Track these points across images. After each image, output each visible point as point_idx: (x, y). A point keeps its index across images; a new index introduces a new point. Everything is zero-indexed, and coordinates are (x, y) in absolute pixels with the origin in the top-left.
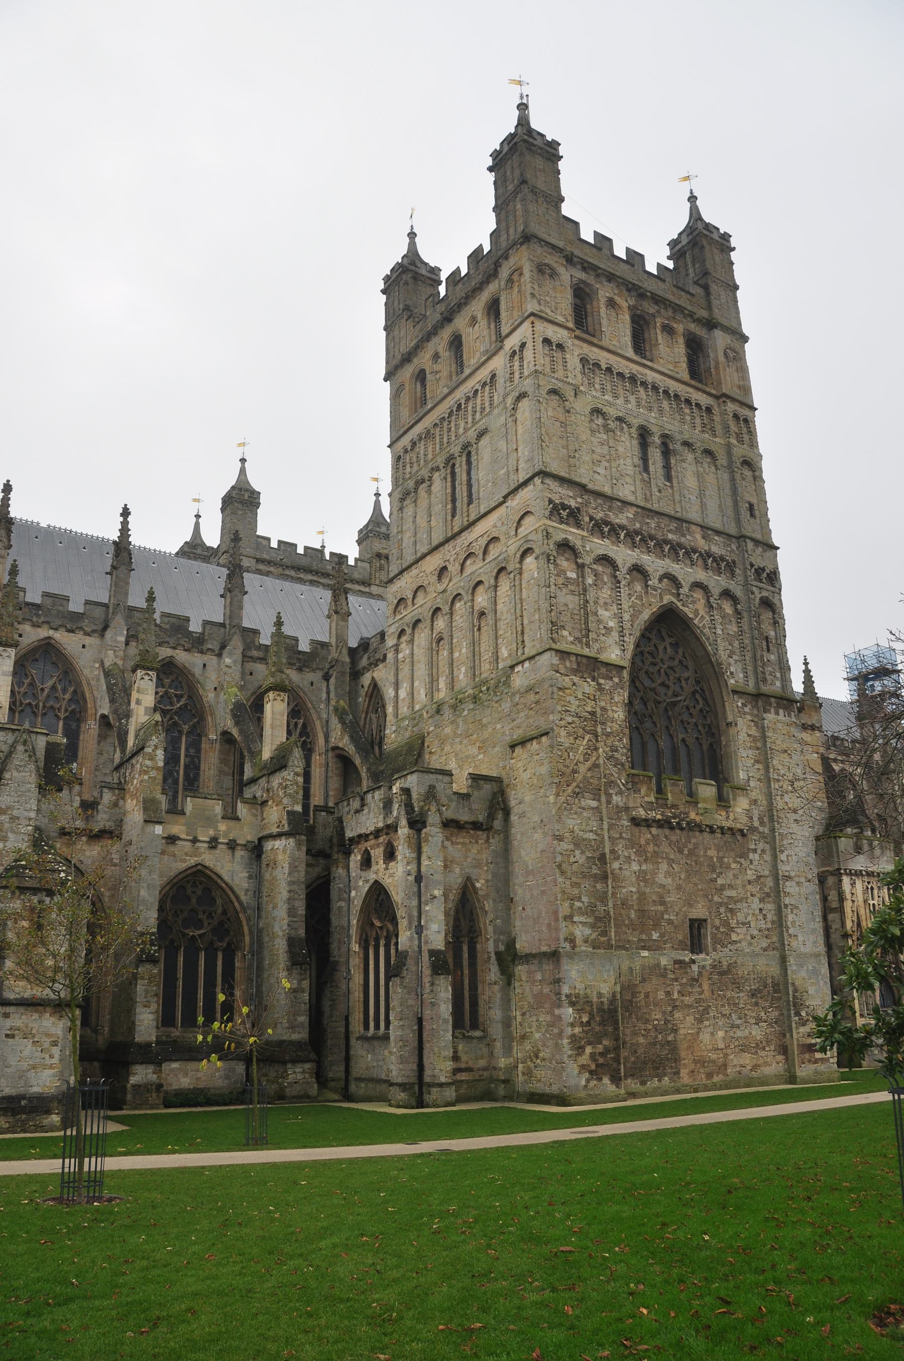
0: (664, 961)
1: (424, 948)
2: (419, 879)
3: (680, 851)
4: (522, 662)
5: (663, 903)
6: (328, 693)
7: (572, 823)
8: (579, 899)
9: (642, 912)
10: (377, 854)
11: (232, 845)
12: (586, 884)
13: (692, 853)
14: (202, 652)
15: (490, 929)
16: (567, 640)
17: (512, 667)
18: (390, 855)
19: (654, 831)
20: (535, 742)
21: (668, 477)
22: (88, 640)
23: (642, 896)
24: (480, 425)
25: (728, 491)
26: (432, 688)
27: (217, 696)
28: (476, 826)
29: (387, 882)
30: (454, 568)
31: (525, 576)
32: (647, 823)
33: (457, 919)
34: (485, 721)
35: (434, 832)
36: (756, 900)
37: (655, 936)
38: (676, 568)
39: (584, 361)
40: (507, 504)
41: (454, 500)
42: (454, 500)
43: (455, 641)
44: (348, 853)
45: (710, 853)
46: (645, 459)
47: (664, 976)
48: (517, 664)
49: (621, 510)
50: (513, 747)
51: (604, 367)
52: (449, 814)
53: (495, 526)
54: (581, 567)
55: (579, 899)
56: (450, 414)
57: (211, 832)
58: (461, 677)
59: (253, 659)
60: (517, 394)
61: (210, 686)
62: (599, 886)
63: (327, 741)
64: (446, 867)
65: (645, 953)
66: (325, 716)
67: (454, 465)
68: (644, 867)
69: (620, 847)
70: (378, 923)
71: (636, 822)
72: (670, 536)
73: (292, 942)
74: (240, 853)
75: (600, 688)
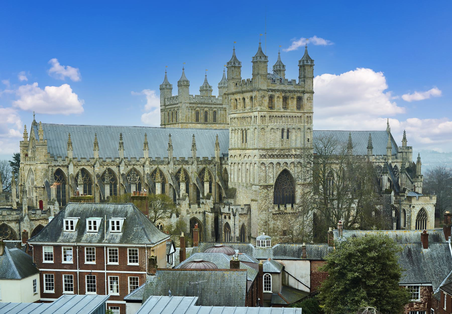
0: (277, 238)
1: (236, 236)
2: (235, 225)
3: (282, 218)
5: (278, 228)
6: (215, 169)
7: (261, 216)
8: (261, 229)
9: (274, 230)
10: (227, 217)
11: (200, 213)
12: (263, 226)
13: (285, 218)
14: (188, 165)
15: (247, 232)
16: (262, 183)
18: (230, 218)
19: (277, 215)
21: (288, 138)
22: (165, 166)
23: (274, 227)
25: (303, 137)
26: (238, 180)
27: (192, 174)
28: (245, 214)
29: (229, 223)
32: (276, 214)
33: (241, 231)
35: (237, 216)
36: (298, 225)
37: (276, 234)
38: (286, 160)
39: (270, 116)
41: (243, 139)
42: (243, 139)
44: (222, 215)
45: (289, 218)
46: (282, 137)
47: (277, 241)
49: (275, 151)
51: (275, 116)
52: (240, 213)
54: (266, 167)
55: (261, 229)
57: (196, 211)
59: (199, 164)
61: (190, 172)
62: (265, 227)
63: (215, 181)
64: (239, 222)
65: (274, 237)
66: (214, 174)
68: (275, 222)
69: (270, 219)
70: (227, 229)
71: (273, 214)
72: (286, 153)
73: (212, 232)
74: (201, 214)
75: (268, 190)
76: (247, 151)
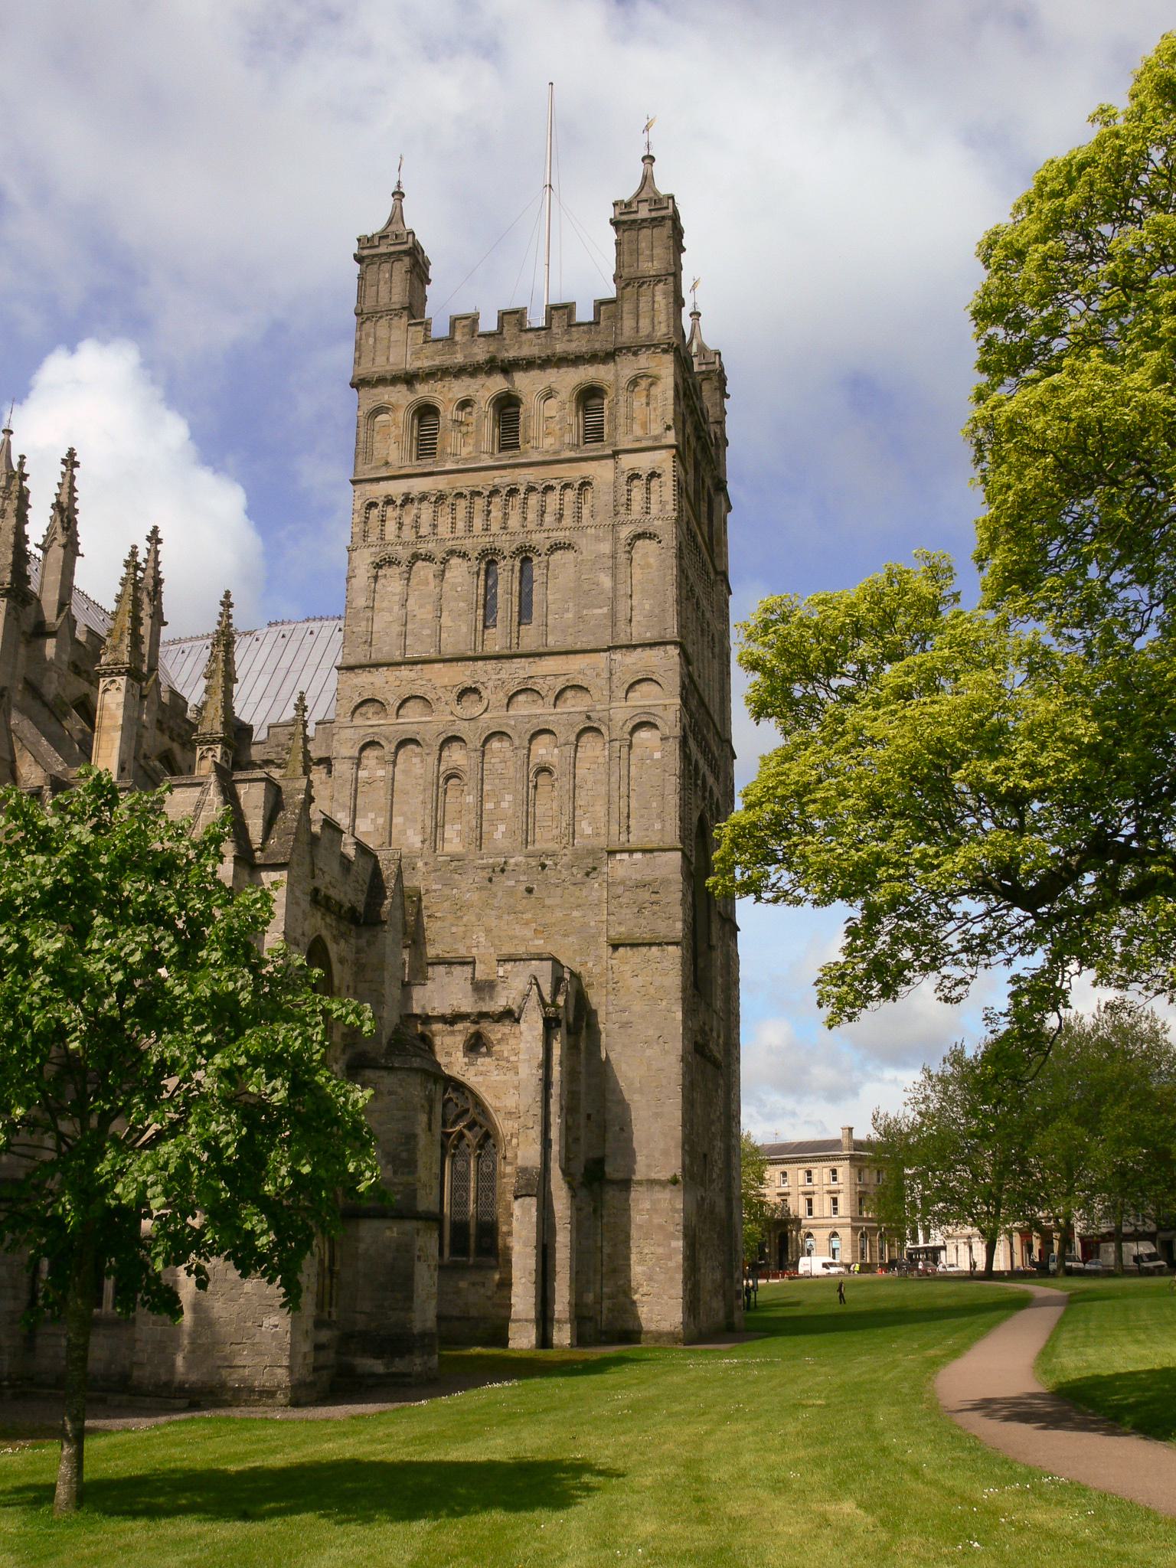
4: (631, 852)
17: (612, 853)
20: (654, 949)
24: (560, 536)
30: (494, 696)
31: (636, 751)
34: (548, 902)
40: (613, 657)
43: (486, 787)
48: (622, 851)
50: (615, 947)
53: (581, 672)
56: (495, 492)
58: (498, 835)
60: (640, 530)
67: (492, 562)
76: (549, 665)
